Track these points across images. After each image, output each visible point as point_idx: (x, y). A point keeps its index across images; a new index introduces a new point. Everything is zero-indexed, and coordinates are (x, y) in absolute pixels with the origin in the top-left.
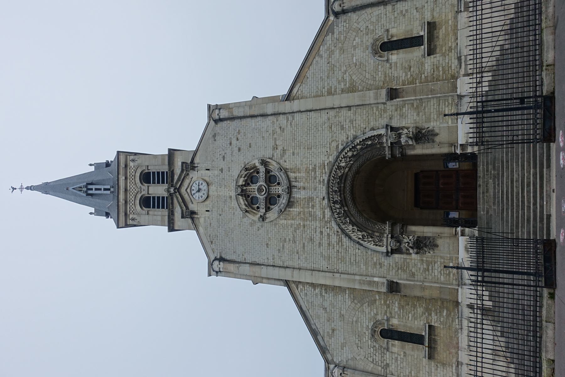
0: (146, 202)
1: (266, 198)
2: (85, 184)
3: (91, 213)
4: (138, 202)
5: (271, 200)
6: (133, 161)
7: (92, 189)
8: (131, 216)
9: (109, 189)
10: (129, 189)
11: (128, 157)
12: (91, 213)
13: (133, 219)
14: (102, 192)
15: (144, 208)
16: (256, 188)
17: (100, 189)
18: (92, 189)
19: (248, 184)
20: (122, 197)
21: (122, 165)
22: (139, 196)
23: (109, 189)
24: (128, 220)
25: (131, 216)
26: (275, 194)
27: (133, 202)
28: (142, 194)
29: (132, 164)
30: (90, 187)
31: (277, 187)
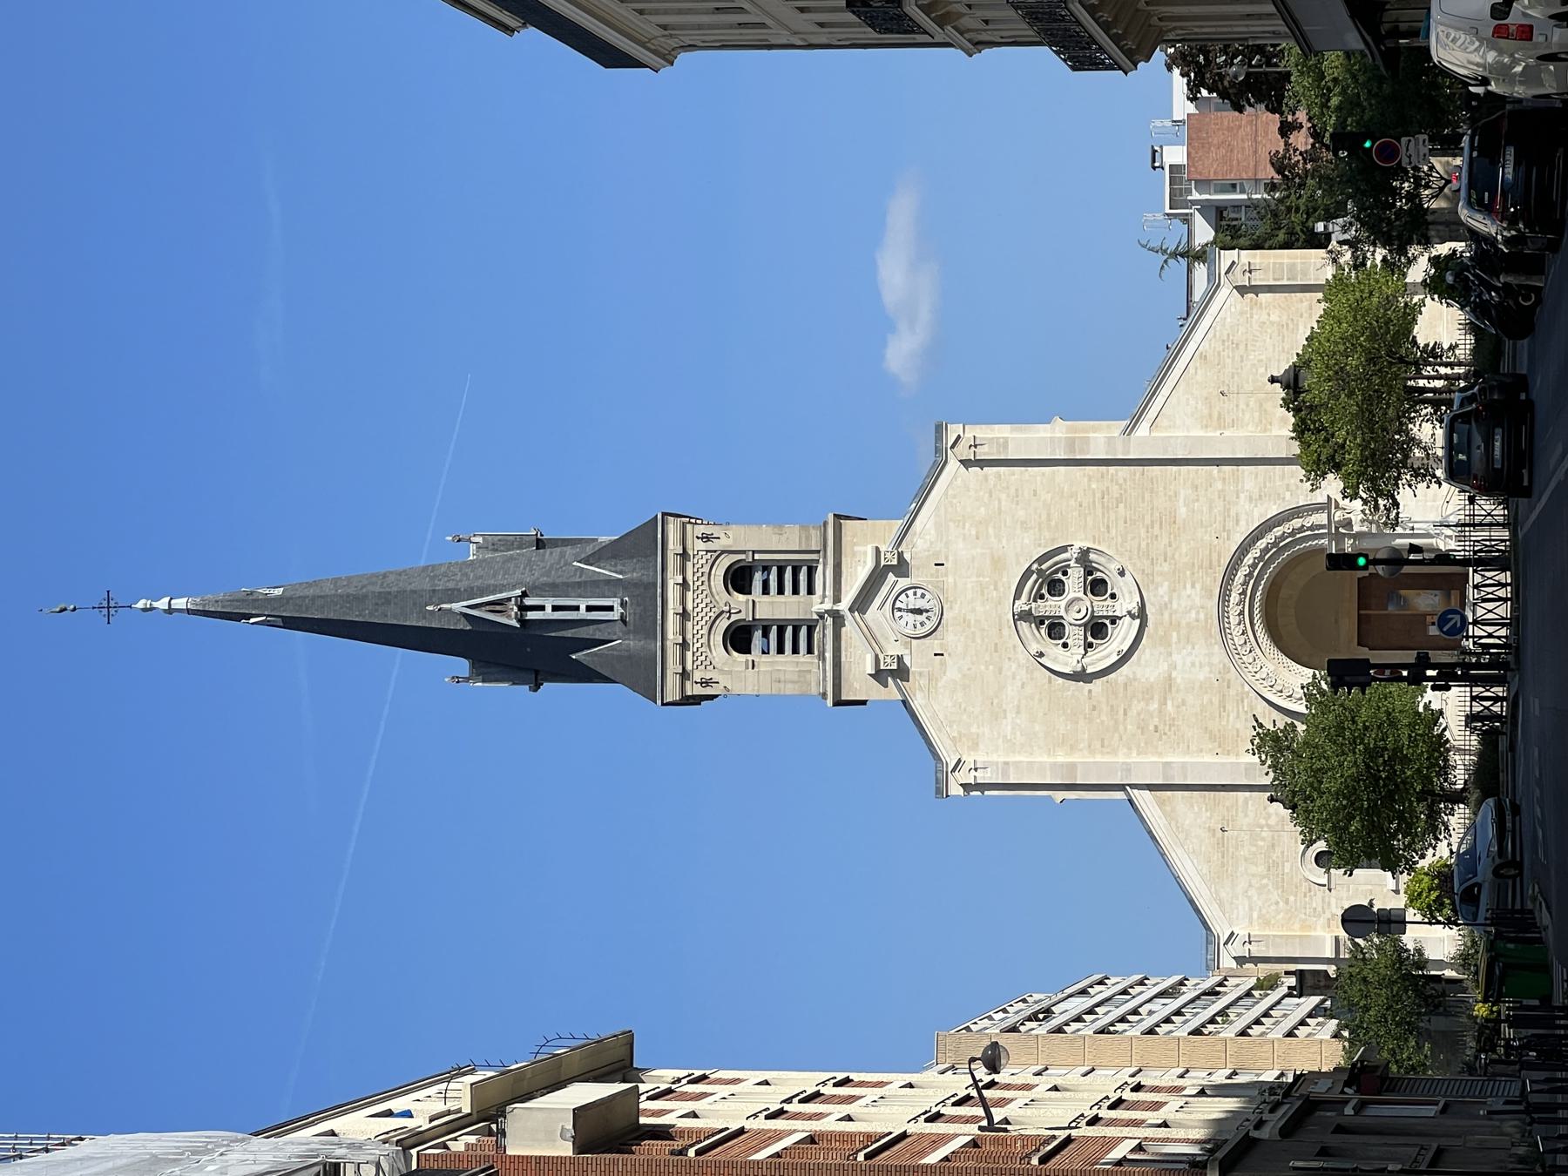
0: (739, 638)
1: (1085, 625)
2: (518, 592)
3: (457, 679)
4: (718, 638)
5: (1097, 629)
6: (706, 538)
7: (542, 608)
8: (697, 676)
9: (611, 608)
10: (690, 607)
11: (689, 527)
12: (457, 679)
13: (706, 683)
14: (583, 614)
15: (735, 654)
16: (1063, 604)
17: (577, 608)
18: (542, 608)
19: (1042, 597)
20: (672, 623)
21: (671, 546)
22: (723, 624)
23: (611, 608)
24: (688, 684)
25: (697, 676)
26: (1106, 617)
27: (704, 640)
28: (734, 618)
29: (700, 545)
30: (528, 602)
31: (1110, 602)
